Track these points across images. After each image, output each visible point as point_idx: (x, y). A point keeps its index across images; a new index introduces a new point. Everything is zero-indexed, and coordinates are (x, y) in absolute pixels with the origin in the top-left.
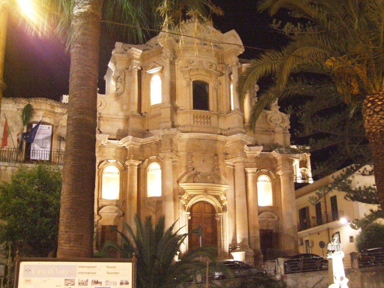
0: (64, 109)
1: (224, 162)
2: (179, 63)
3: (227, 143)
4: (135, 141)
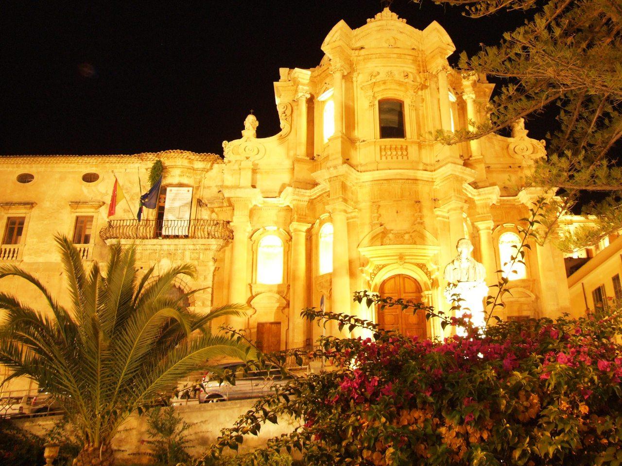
0: (206, 163)
1: (433, 213)
2: (360, 78)
3: (435, 184)
4: (298, 195)
